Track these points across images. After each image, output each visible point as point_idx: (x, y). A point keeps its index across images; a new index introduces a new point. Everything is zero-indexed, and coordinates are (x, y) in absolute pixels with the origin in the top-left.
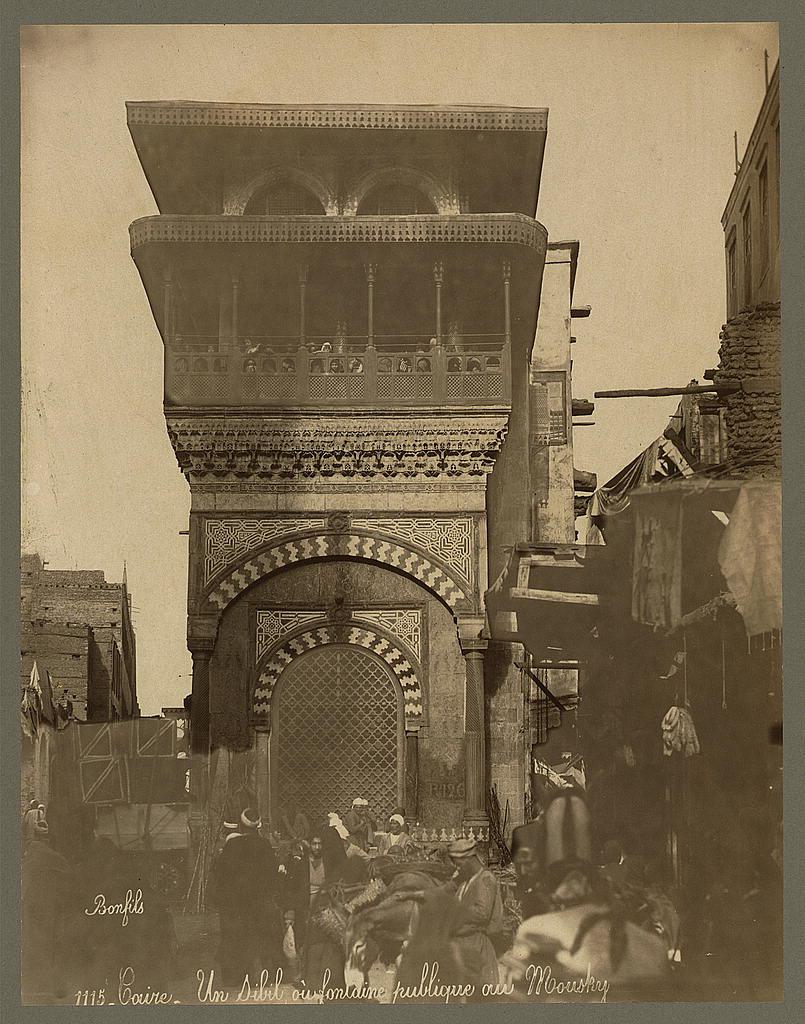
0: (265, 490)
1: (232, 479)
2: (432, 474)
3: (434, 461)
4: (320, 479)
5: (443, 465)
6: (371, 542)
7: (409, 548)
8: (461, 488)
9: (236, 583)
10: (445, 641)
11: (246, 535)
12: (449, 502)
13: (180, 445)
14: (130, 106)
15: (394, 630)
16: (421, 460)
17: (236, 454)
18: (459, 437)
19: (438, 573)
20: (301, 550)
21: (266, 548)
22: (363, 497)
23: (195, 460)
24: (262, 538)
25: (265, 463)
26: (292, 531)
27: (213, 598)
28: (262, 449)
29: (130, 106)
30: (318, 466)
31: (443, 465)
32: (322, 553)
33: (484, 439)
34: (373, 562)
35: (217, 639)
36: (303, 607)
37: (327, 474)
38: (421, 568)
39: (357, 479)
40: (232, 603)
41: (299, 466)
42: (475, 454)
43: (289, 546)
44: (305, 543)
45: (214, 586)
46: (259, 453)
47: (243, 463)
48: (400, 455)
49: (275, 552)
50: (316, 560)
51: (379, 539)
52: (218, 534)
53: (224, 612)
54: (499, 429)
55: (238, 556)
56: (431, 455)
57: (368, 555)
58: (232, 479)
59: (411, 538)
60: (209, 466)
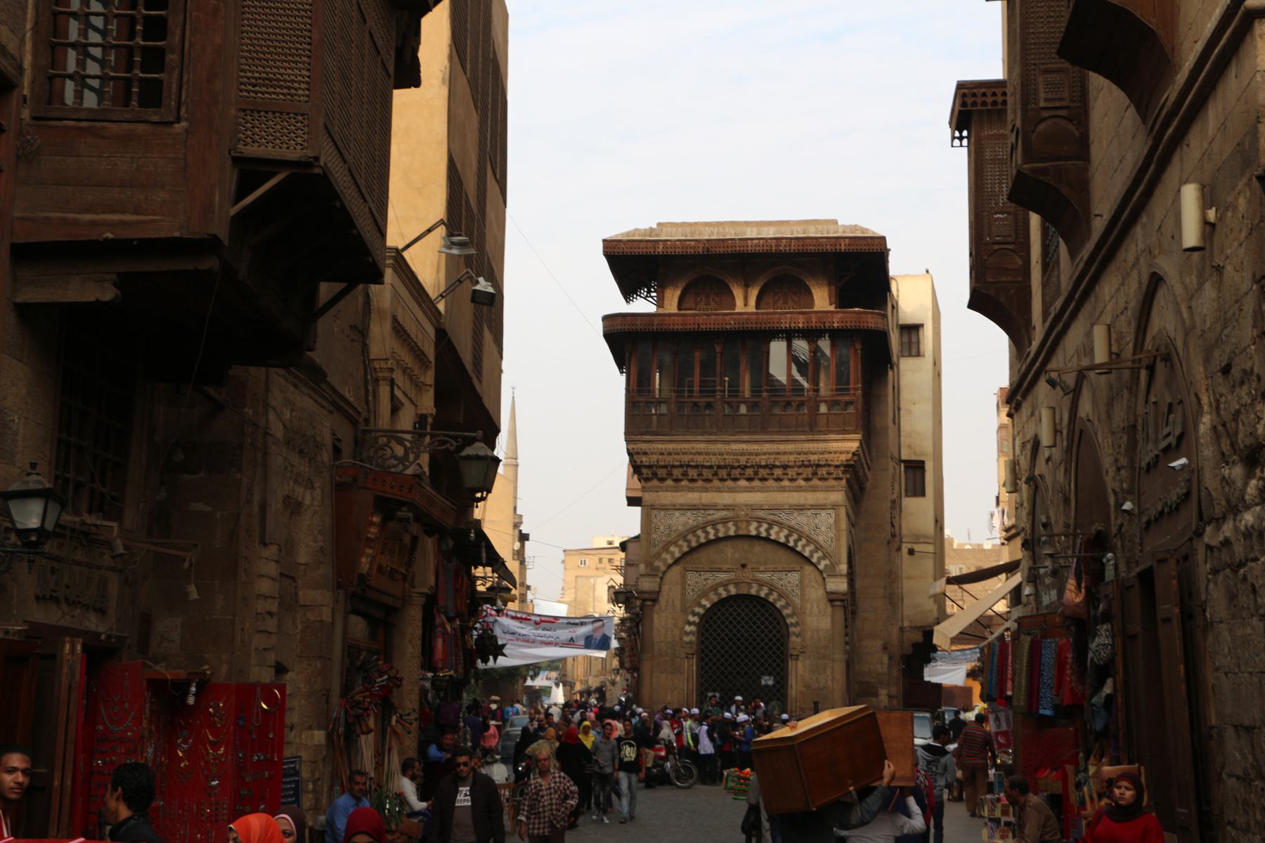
0: (691, 490)
1: (669, 482)
2: (807, 480)
3: (810, 470)
4: (729, 483)
5: (815, 474)
6: (765, 526)
7: (792, 530)
8: (828, 489)
9: (672, 554)
10: (816, 594)
11: (681, 521)
12: (819, 497)
14: (604, 241)
16: (800, 471)
17: (674, 467)
19: (812, 547)
20: (717, 531)
21: (693, 531)
22: (759, 494)
23: (644, 471)
25: (693, 473)
26: (710, 518)
27: (657, 563)
29: (604, 241)
30: (729, 475)
31: (815, 474)
32: (732, 533)
33: (843, 457)
34: (767, 539)
35: (659, 592)
36: (719, 570)
37: (735, 480)
38: (800, 544)
39: (756, 483)
40: (670, 566)
41: (716, 474)
42: (837, 466)
43: (709, 529)
44: (720, 527)
45: (658, 556)
46: (689, 466)
48: (785, 467)
49: (699, 533)
50: (727, 538)
52: (660, 519)
53: (664, 573)
55: (674, 535)
56: (806, 466)
57: (764, 534)
58: (669, 482)
59: (793, 523)
60: (655, 474)
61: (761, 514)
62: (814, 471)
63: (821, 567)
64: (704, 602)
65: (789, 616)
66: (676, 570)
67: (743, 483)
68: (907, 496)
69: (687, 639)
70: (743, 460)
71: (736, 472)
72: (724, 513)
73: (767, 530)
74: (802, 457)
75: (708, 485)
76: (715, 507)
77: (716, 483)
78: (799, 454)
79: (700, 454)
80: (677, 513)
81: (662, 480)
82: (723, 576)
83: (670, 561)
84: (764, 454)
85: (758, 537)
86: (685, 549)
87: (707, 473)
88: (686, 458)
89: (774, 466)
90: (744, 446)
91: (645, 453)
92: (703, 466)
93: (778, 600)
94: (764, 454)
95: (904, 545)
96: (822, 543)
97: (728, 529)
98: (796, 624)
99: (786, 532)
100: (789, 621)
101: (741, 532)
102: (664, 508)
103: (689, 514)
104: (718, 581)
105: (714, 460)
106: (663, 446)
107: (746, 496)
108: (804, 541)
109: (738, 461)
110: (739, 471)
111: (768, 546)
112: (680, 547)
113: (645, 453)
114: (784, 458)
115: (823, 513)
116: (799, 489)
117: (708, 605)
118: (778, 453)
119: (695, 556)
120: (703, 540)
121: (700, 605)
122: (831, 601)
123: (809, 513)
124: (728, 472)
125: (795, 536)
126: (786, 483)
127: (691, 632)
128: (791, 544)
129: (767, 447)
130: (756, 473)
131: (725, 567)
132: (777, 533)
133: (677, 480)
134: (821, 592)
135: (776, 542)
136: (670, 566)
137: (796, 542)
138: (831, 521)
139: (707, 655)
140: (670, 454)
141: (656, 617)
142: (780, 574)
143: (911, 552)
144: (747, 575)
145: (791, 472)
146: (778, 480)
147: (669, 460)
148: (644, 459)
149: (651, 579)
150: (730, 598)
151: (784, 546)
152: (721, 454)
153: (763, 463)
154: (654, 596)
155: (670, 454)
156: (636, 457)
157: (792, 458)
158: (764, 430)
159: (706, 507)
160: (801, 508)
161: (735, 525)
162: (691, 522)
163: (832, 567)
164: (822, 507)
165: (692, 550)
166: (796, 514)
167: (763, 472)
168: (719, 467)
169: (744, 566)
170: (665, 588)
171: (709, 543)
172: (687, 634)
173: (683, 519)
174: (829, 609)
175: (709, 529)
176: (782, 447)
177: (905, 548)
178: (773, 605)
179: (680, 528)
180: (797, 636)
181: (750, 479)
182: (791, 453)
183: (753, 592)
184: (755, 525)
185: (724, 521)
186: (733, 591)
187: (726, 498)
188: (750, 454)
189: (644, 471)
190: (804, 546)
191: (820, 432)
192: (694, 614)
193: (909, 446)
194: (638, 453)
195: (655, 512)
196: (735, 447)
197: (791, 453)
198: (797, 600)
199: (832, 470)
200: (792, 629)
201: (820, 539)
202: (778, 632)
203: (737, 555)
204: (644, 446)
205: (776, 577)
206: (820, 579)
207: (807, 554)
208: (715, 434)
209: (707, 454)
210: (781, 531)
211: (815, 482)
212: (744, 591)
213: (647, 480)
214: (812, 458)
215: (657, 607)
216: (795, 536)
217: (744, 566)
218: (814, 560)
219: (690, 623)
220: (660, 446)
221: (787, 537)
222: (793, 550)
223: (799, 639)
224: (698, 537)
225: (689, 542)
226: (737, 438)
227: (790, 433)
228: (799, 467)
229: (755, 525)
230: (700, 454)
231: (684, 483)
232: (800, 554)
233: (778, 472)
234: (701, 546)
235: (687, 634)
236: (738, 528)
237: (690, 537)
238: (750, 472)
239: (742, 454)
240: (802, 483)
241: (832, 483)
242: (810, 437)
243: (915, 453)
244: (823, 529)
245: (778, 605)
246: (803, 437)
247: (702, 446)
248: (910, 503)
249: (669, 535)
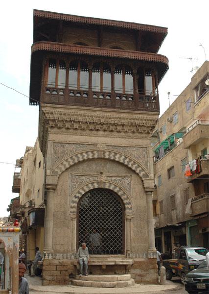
1: (63, 130)
5: (137, 130)
13: (46, 117)
18: (144, 122)
19: (136, 165)
20: (88, 155)
25: (76, 126)
27: (56, 170)
28: (76, 120)
30: (95, 128)
31: (137, 130)
34: (114, 161)
37: (98, 130)
38: (130, 163)
39: (108, 133)
40: (63, 172)
41: (88, 127)
42: (148, 127)
46: (74, 121)
47: (68, 125)
48: (123, 125)
49: (79, 155)
50: (93, 159)
51: (116, 154)
58: (63, 130)
60: (56, 125)
62: (138, 129)
63: (141, 175)
65: (125, 199)
66: (67, 175)
67: (101, 133)
70: (102, 121)
71: (98, 127)
74: (132, 121)
75: (84, 132)
77: (88, 132)
78: (130, 119)
79: (81, 115)
80: (67, 145)
81: (60, 128)
83: (64, 169)
84: (114, 118)
85: (109, 160)
86: (72, 163)
87: (83, 126)
88: (73, 118)
89: (118, 125)
90: (104, 113)
91: (52, 113)
92: (82, 122)
94: (114, 118)
98: (129, 203)
100: (125, 202)
101: (100, 157)
103: (73, 146)
105: (88, 120)
106: (62, 110)
107: (103, 140)
109: (100, 120)
110: (100, 126)
111: (115, 166)
113: (52, 113)
114: (123, 121)
115: (141, 149)
116: (130, 137)
118: (120, 118)
119: (76, 167)
120: (81, 159)
121: (79, 192)
122: (146, 192)
123: (134, 149)
124: (95, 127)
125: (128, 160)
126: (122, 134)
127: (74, 207)
128: (126, 163)
129: (115, 115)
130: (109, 127)
133: (68, 129)
134: (141, 187)
135: (118, 162)
136: (63, 172)
137: (129, 162)
138: (145, 153)
139: (82, 219)
140: (64, 115)
144: (104, 178)
145: (126, 129)
146: (119, 132)
147: (66, 118)
148: (51, 116)
150: (94, 189)
151: (122, 164)
152: (92, 117)
153: (113, 123)
154: (54, 187)
155: (64, 115)
156: (46, 115)
163: (147, 175)
165: (75, 164)
167: (112, 128)
168: (90, 123)
169: (101, 173)
170: (60, 183)
171: (84, 161)
172: (72, 207)
174: (145, 196)
175: (84, 154)
176: (122, 115)
178: (116, 193)
180: (131, 209)
181: (105, 131)
182: (127, 119)
183: (107, 187)
186: (96, 186)
187: (92, 139)
188: (107, 118)
189: (51, 123)
190: (132, 165)
191: (140, 110)
192: (76, 197)
194: (48, 113)
195: (55, 144)
196: (98, 113)
197: (127, 119)
199: (145, 128)
200: (127, 206)
204: (51, 110)
206: (140, 182)
207: (134, 168)
209: (85, 116)
211: (137, 134)
212: (102, 186)
213: (52, 127)
214: (136, 121)
216: (128, 160)
217: (101, 173)
218: (138, 171)
219: (73, 202)
220: (60, 110)
221: (124, 160)
222: (126, 166)
224: (78, 158)
226: (100, 109)
228: (130, 126)
229: (107, 153)
230: (81, 115)
231: (71, 131)
232: (130, 169)
233: (119, 128)
234: (79, 162)
235: (72, 207)
238: (105, 127)
239: (103, 117)
240: (131, 134)
241: (145, 135)
245: (119, 194)
246: (133, 112)
247: (82, 112)
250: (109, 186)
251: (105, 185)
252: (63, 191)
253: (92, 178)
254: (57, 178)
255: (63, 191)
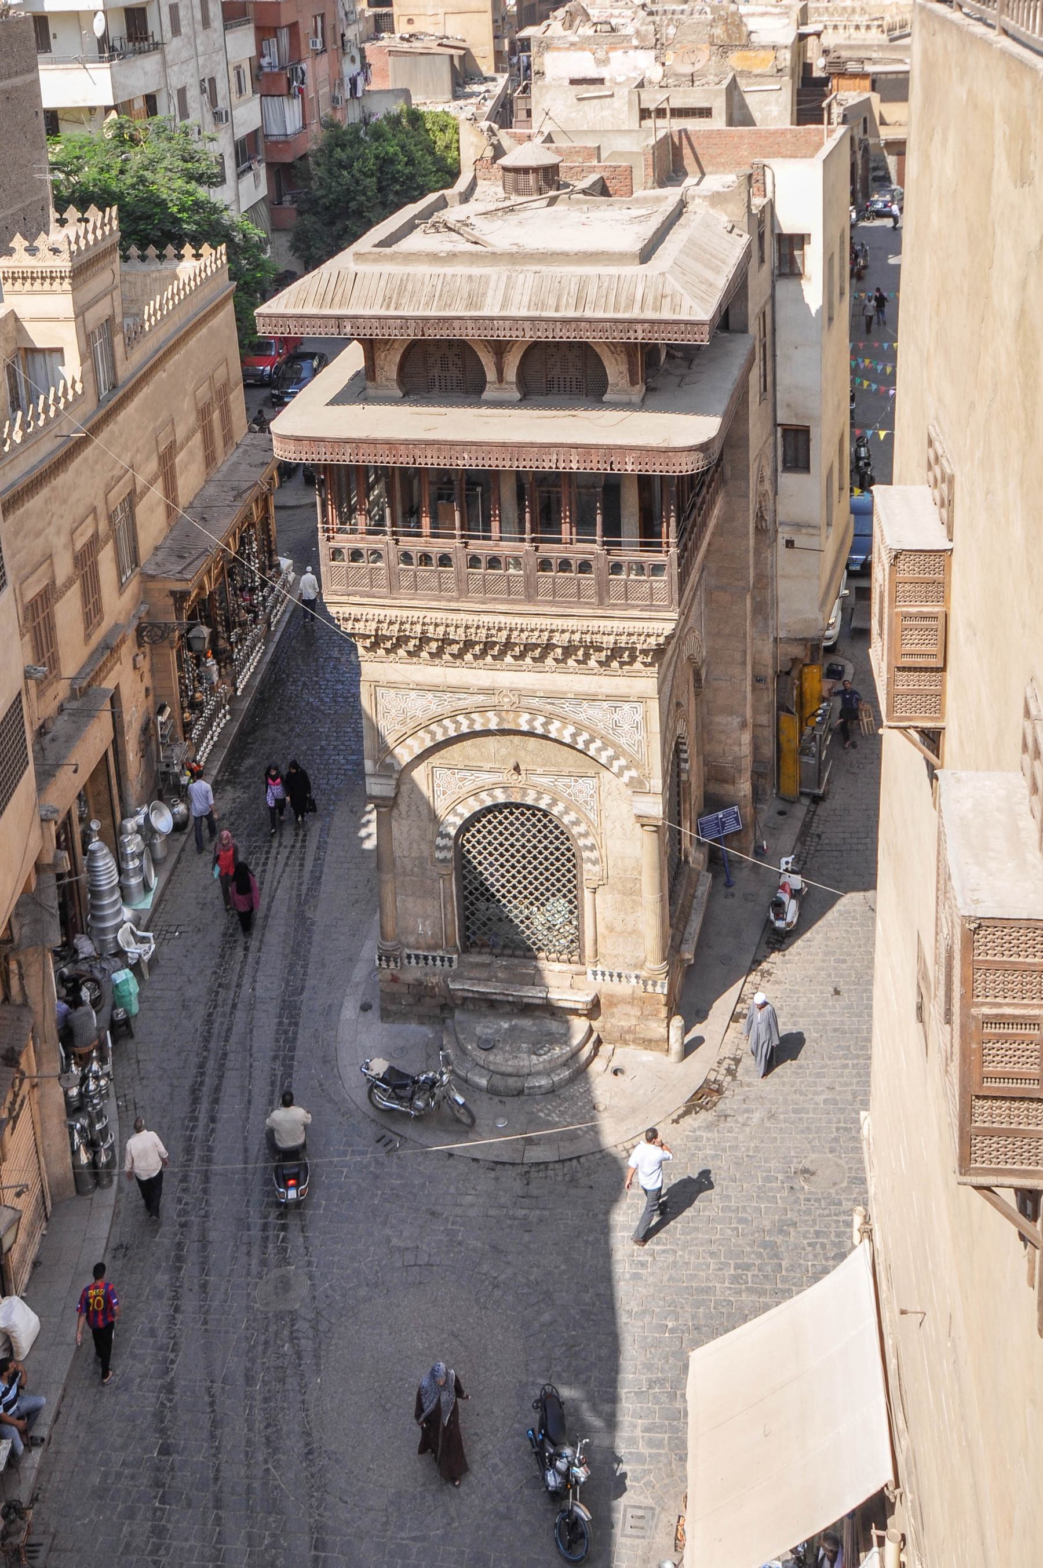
6: (541, 720)
15: (570, 795)
24: (435, 709)
26: (462, 704)
32: (493, 726)
33: (652, 641)
36: (479, 769)
38: (593, 747)
50: (487, 733)
54: (666, 633)
57: (540, 730)
59: (583, 716)
61: (535, 703)
64: (460, 809)
68: (786, 469)
69: (439, 855)
72: (482, 697)
73: (545, 725)
76: (466, 690)
80: (413, 694)
82: (486, 779)
85: (531, 734)
86: (429, 743)
93: (566, 812)
95: (780, 536)
96: (625, 747)
97: (488, 720)
98: (592, 848)
99: (571, 729)
102: (392, 685)
104: (480, 784)
106: (383, 612)
108: (598, 743)
112: (423, 740)
115: (626, 706)
117: (467, 815)
123: (605, 705)
125: (585, 736)
127: (445, 847)
131: (487, 766)
132: (559, 730)
138: (638, 718)
141: (394, 824)
142: (567, 780)
143: (790, 544)
149: (382, 781)
157: (577, 637)
158: (530, 598)
159: (453, 689)
160: (593, 698)
161: (498, 713)
162: (433, 707)
164: (625, 699)
166: (585, 704)
173: (421, 703)
177: (781, 542)
179: (419, 713)
180: (595, 862)
184: (526, 717)
185: (482, 710)
186: (501, 798)
190: (599, 750)
193: (788, 405)
198: (592, 816)
201: (622, 741)
202: (568, 850)
203: (503, 752)
205: (561, 783)
208: (457, 600)
210: (564, 727)
212: (516, 798)
215: (395, 812)
223: (597, 868)
225: (433, 734)
227: (570, 604)
229: (526, 717)
236: (502, 720)
237: (433, 727)
242: (600, 612)
243: (796, 415)
244: (626, 727)
248: (789, 481)
249: (403, 723)
250: (537, 800)
251: (525, 795)
252: (414, 808)
253: (486, 776)
254: (394, 782)
255: (414, 808)
